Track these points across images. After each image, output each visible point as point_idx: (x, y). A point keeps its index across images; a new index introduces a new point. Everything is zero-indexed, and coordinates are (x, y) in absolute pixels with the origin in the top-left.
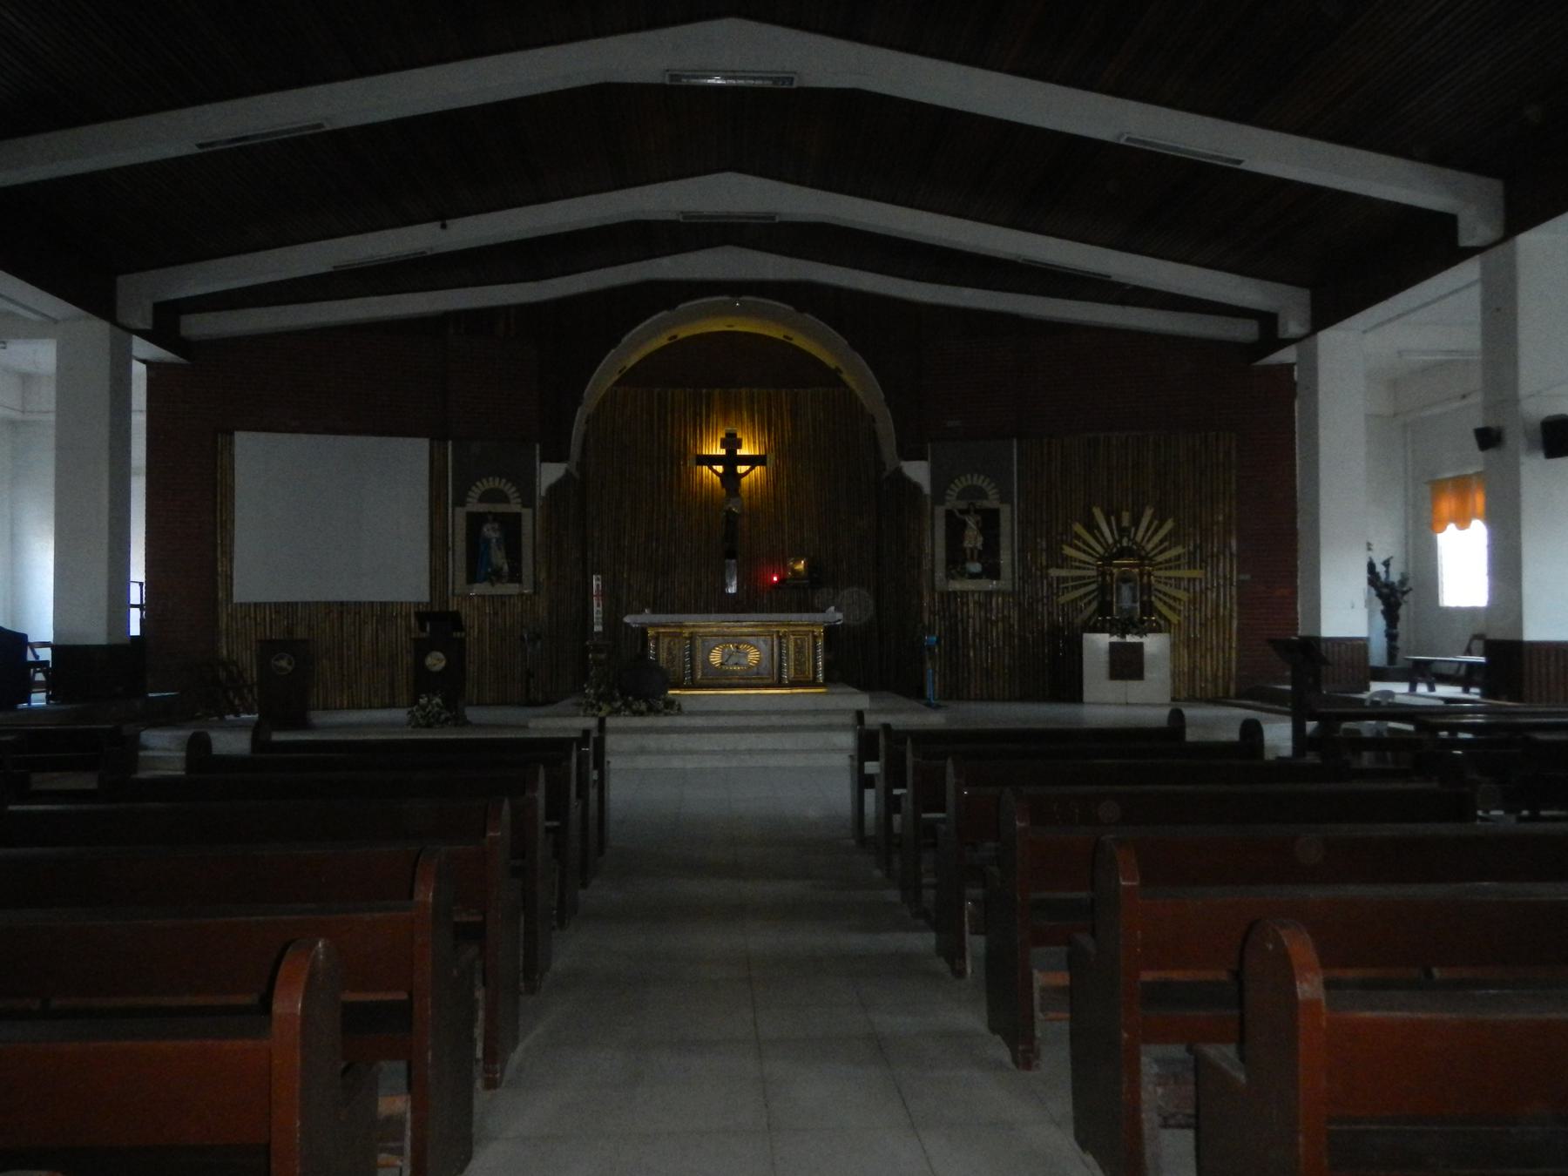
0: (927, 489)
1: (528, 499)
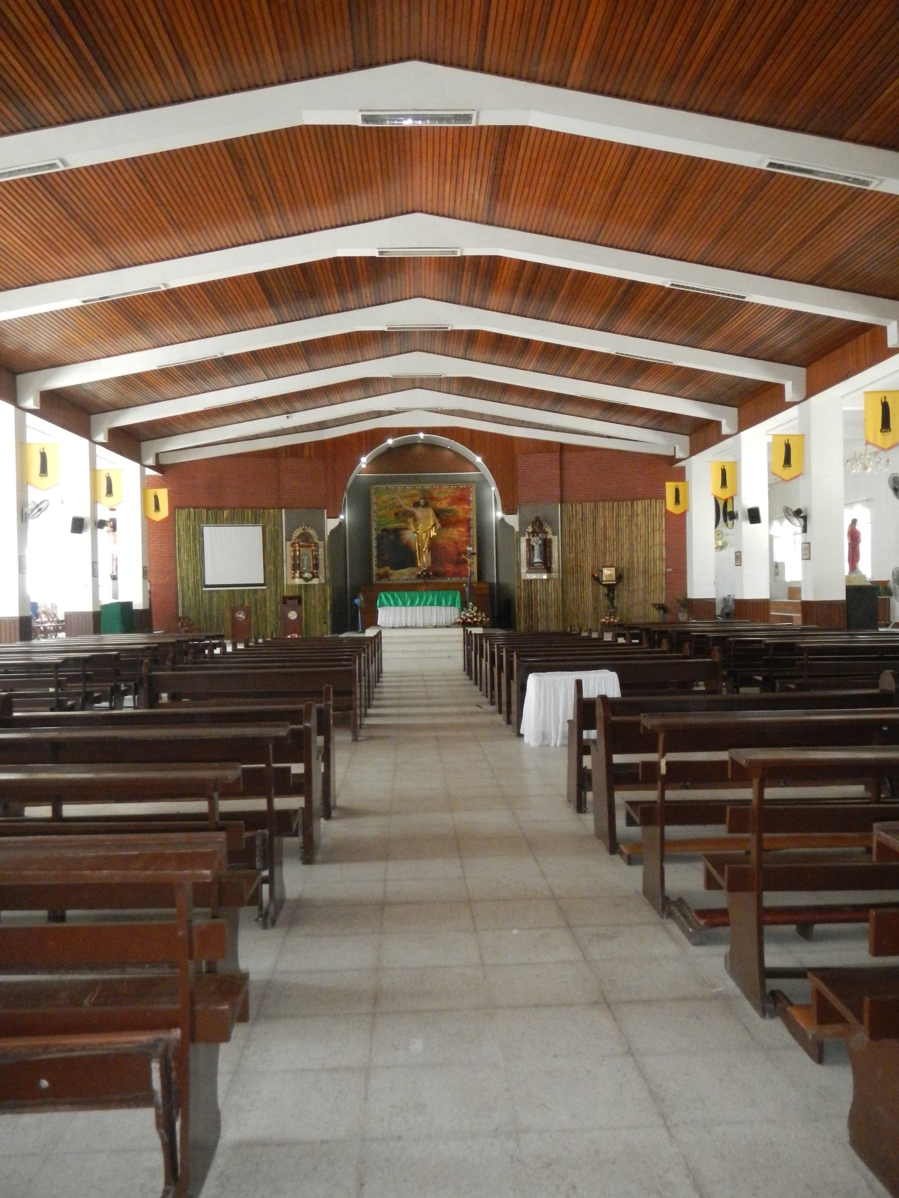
0: (517, 529)
1: (321, 538)
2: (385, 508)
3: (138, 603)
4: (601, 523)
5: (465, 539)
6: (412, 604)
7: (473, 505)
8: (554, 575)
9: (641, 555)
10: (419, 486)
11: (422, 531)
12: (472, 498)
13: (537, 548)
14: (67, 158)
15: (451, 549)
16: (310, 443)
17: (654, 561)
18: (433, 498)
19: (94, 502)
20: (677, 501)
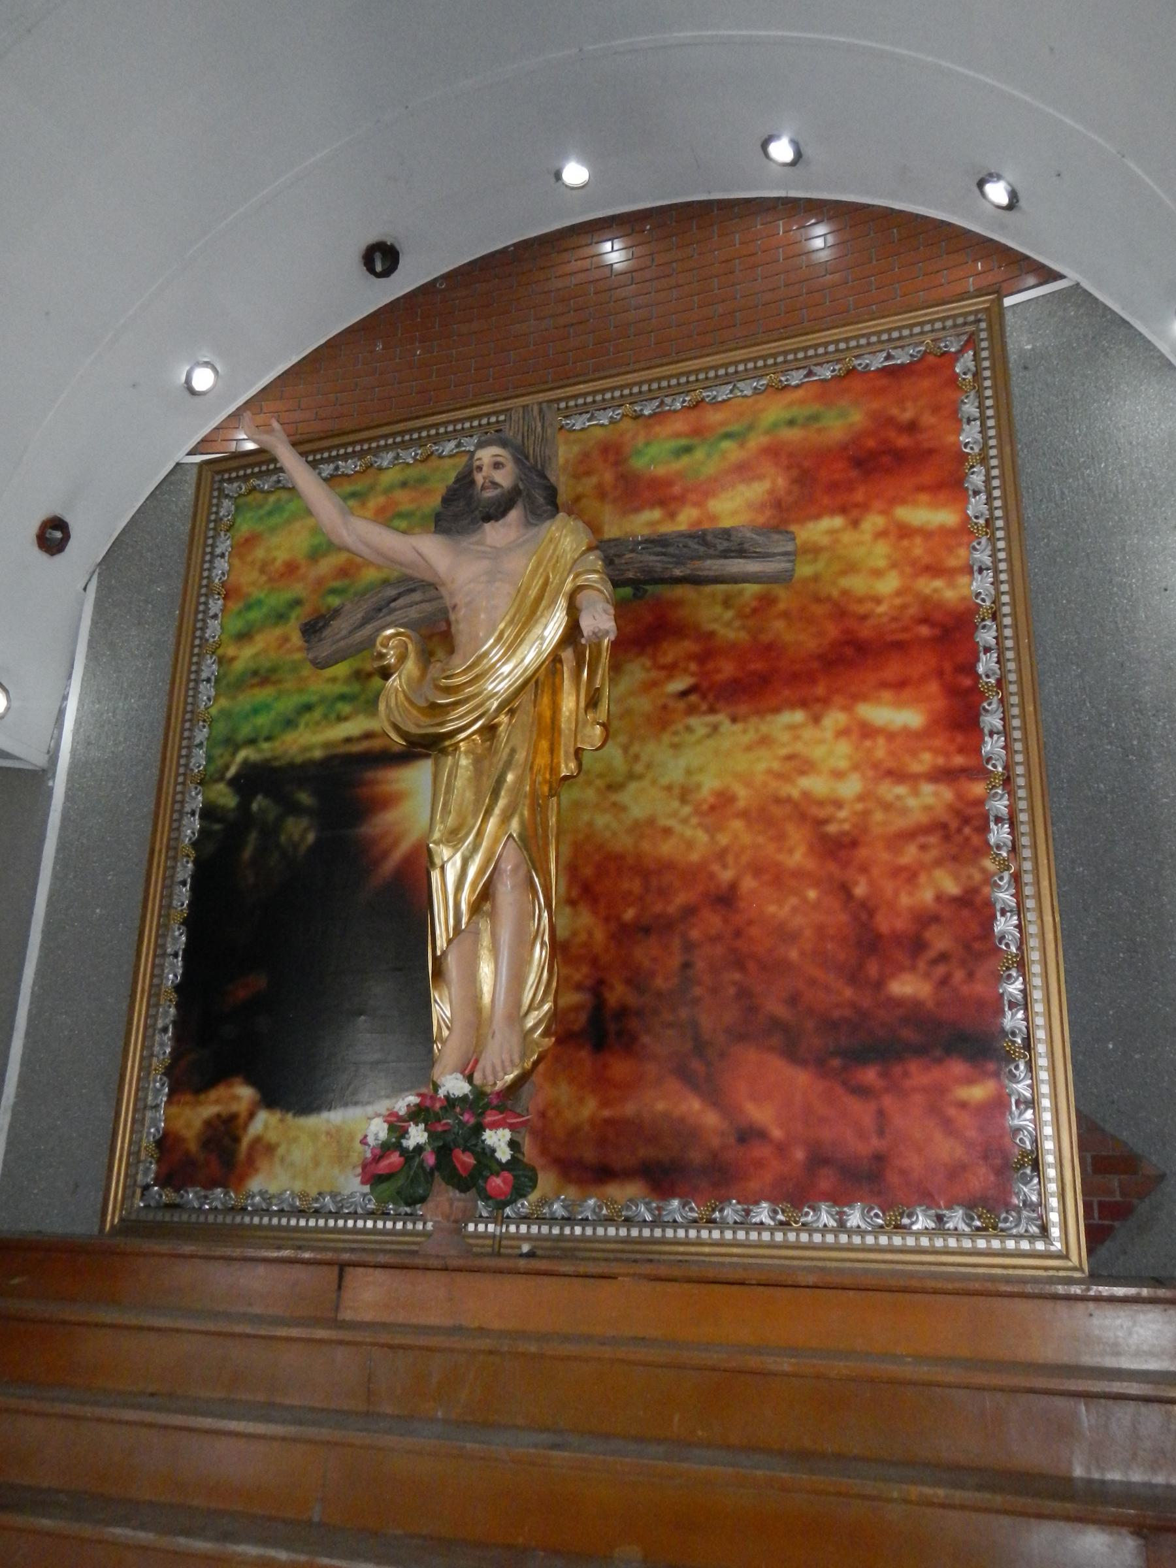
2: (280, 617)
5: (928, 800)
15: (795, 911)
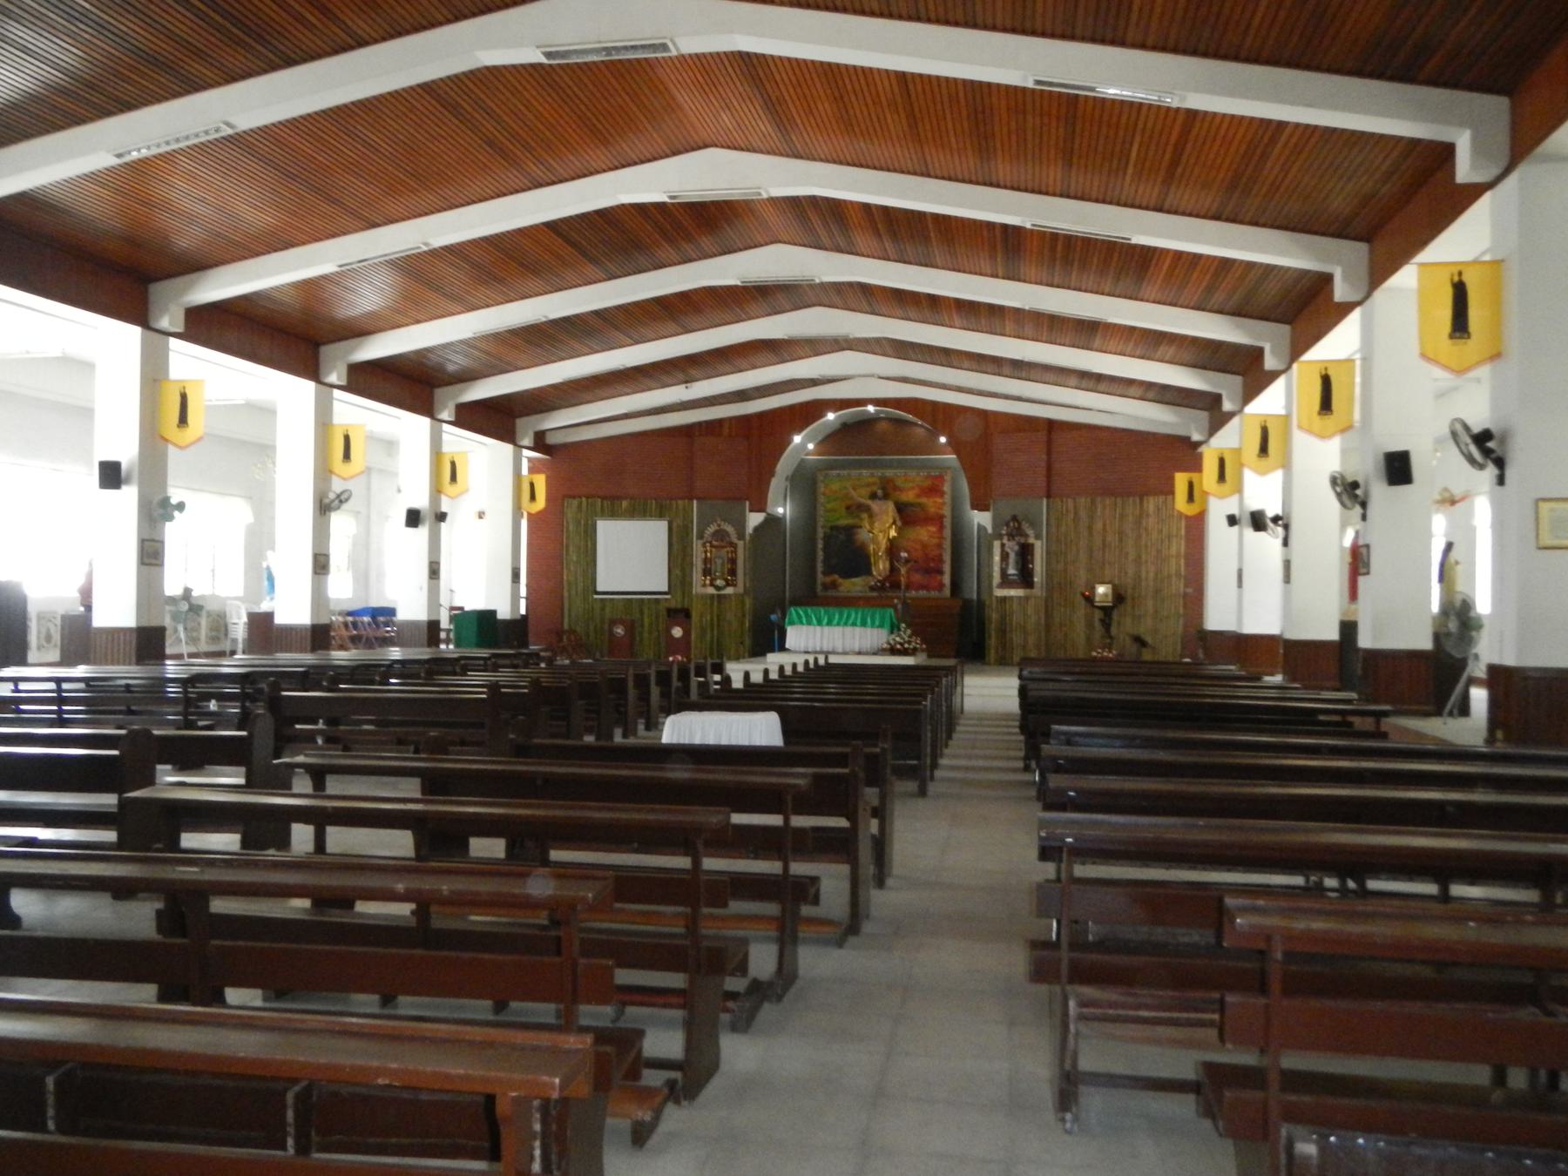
0: (990, 531)
1: (741, 536)
3: (504, 613)
4: (1099, 525)
5: (935, 541)
6: (829, 623)
7: (947, 498)
8: (1038, 591)
9: (1152, 569)
10: (879, 473)
11: (880, 530)
12: (947, 488)
13: (1012, 557)
14: (232, 120)
16: (731, 419)
17: (1169, 576)
18: (896, 488)
19: (436, 491)
20: (1191, 498)
